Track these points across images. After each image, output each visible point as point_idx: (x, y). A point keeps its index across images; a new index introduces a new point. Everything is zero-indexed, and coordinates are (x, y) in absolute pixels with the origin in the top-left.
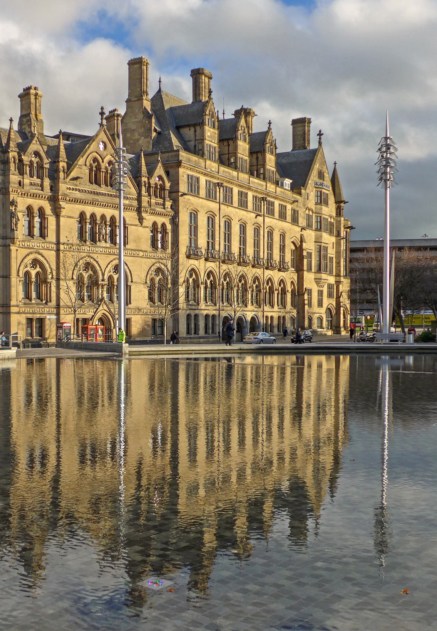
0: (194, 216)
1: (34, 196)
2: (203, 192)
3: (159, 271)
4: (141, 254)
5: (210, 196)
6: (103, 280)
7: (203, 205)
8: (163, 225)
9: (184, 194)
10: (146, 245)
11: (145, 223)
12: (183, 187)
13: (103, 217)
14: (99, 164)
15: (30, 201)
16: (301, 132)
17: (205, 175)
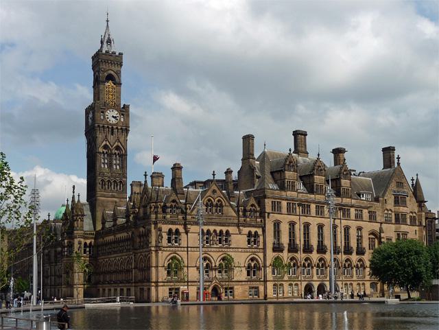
0: (277, 224)
1: (173, 223)
2: (284, 210)
3: (252, 259)
4: (240, 250)
5: (290, 211)
6: (215, 266)
7: (285, 219)
8: (256, 232)
9: (269, 213)
10: (245, 244)
11: (243, 232)
12: (268, 209)
13: (215, 231)
14: (212, 203)
15: (171, 226)
16: (388, 157)
17: (286, 200)
